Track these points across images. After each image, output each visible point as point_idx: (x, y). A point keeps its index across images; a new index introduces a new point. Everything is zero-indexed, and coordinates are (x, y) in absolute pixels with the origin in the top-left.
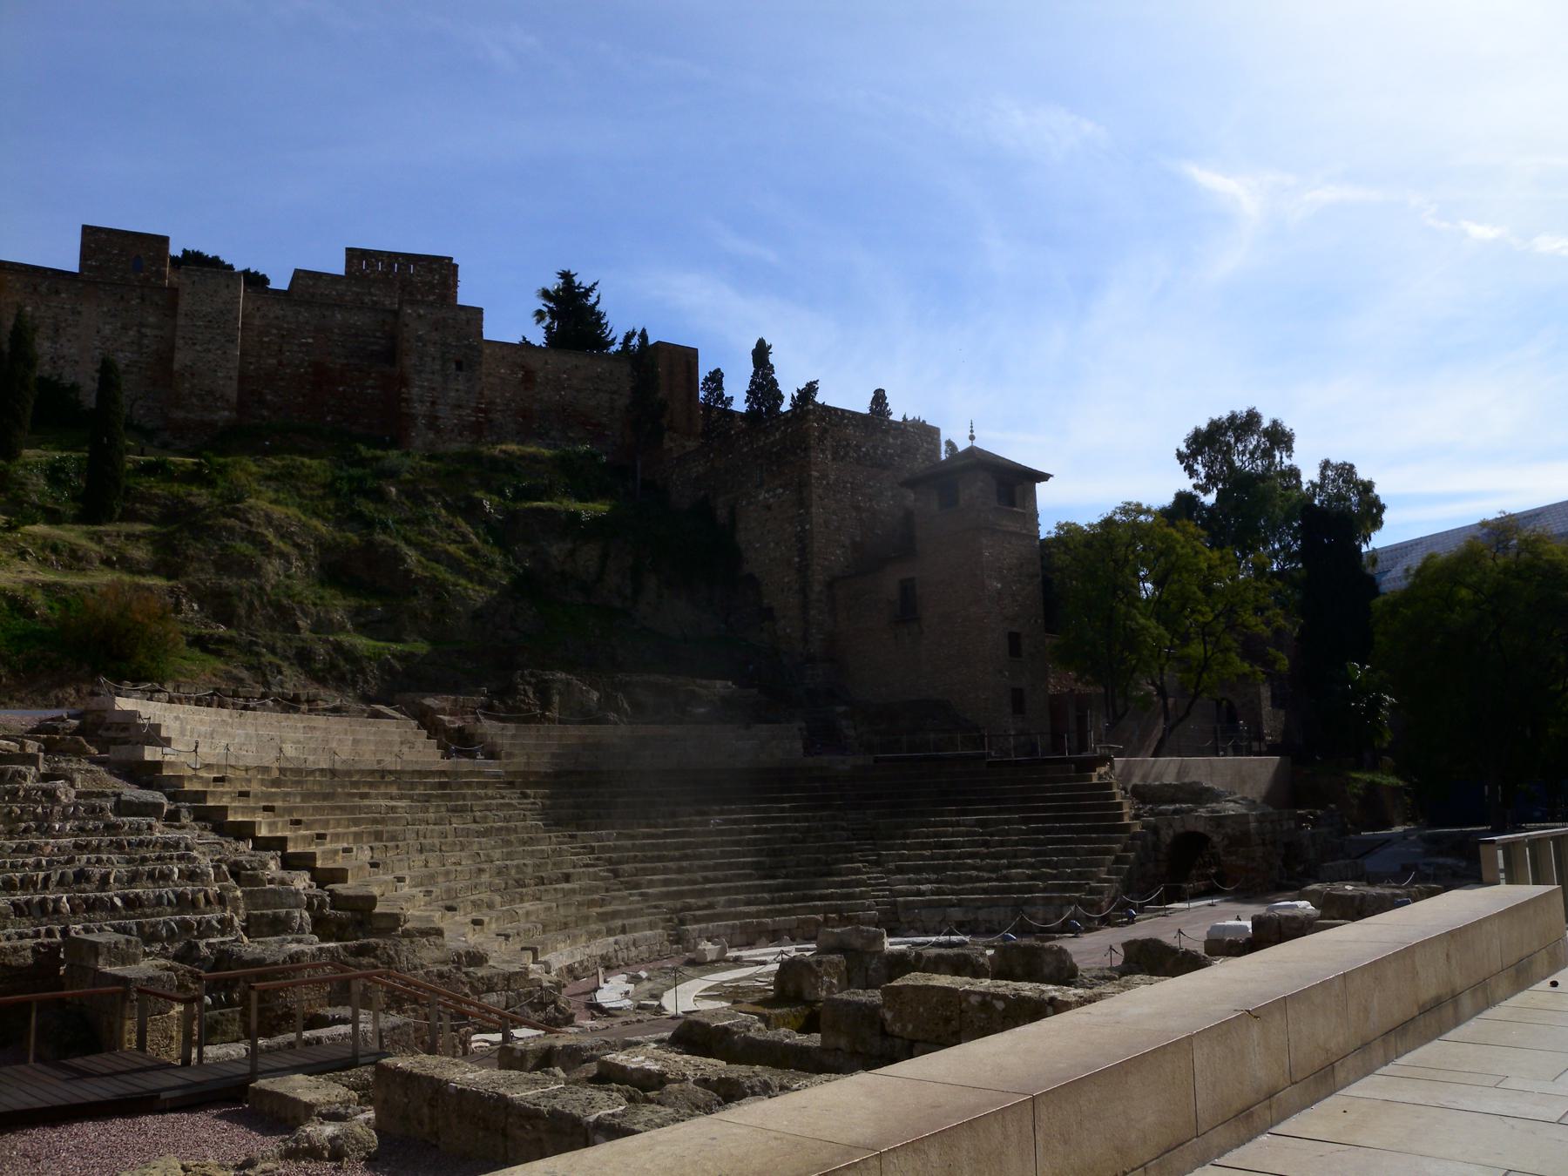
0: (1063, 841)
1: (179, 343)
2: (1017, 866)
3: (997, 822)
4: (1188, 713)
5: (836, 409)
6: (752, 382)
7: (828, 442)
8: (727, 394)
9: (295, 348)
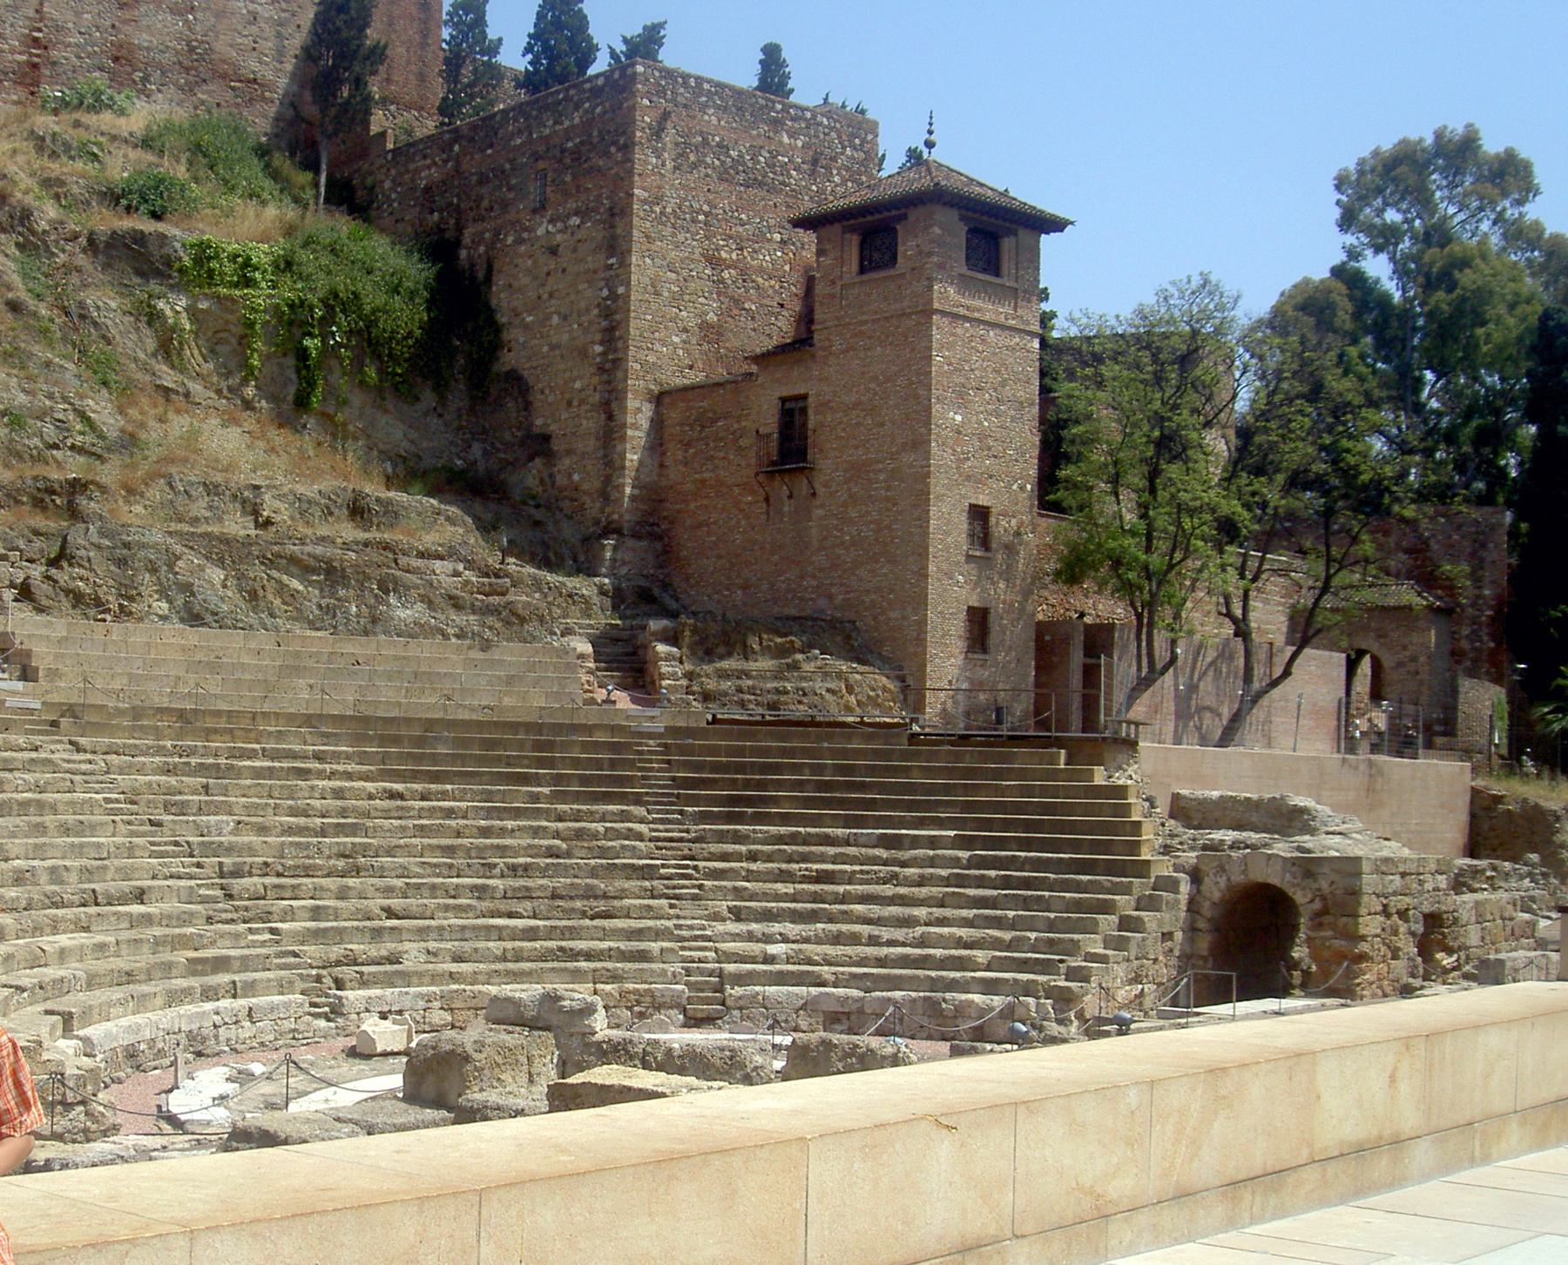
0: (1027, 884)
2: (942, 922)
3: (915, 842)
4: (1287, 673)
5: (685, 77)
6: (540, 16)
7: (670, 136)
8: (492, 34)
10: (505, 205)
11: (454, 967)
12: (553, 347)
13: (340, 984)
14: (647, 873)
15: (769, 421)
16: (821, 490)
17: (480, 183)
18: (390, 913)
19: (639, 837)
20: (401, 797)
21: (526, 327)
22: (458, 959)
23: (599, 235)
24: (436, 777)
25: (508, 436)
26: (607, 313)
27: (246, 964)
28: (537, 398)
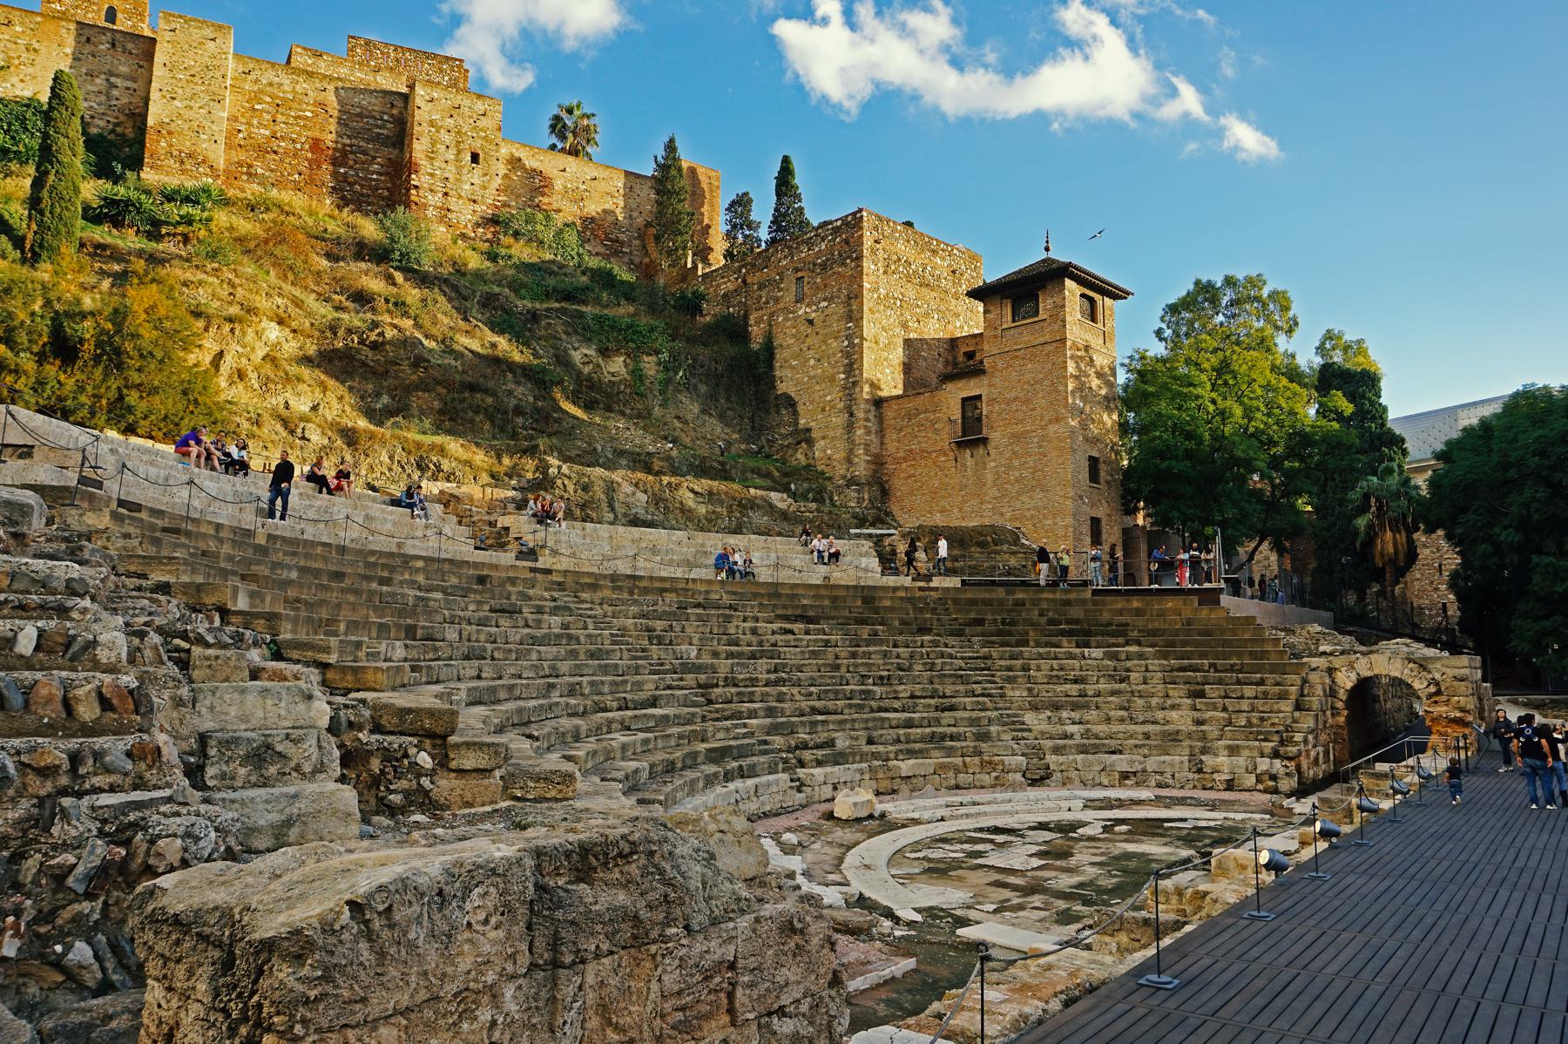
1: (154, 95)
8: (754, 216)
9: (291, 120)
10: (777, 300)
11: (873, 748)
12: (810, 378)
13: (802, 764)
14: (964, 680)
15: (957, 414)
16: (993, 452)
17: (760, 289)
18: (814, 711)
19: (951, 656)
20: (792, 632)
21: (793, 368)
22: (870, 742)
23: (842, 310)
24: (810, 621)
25: (783, 431)
26: (848, 355)
27: (742, 752)
28: (800, 408)
